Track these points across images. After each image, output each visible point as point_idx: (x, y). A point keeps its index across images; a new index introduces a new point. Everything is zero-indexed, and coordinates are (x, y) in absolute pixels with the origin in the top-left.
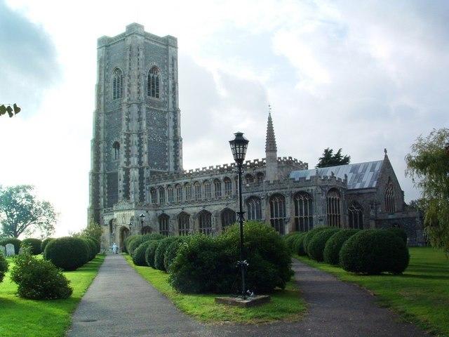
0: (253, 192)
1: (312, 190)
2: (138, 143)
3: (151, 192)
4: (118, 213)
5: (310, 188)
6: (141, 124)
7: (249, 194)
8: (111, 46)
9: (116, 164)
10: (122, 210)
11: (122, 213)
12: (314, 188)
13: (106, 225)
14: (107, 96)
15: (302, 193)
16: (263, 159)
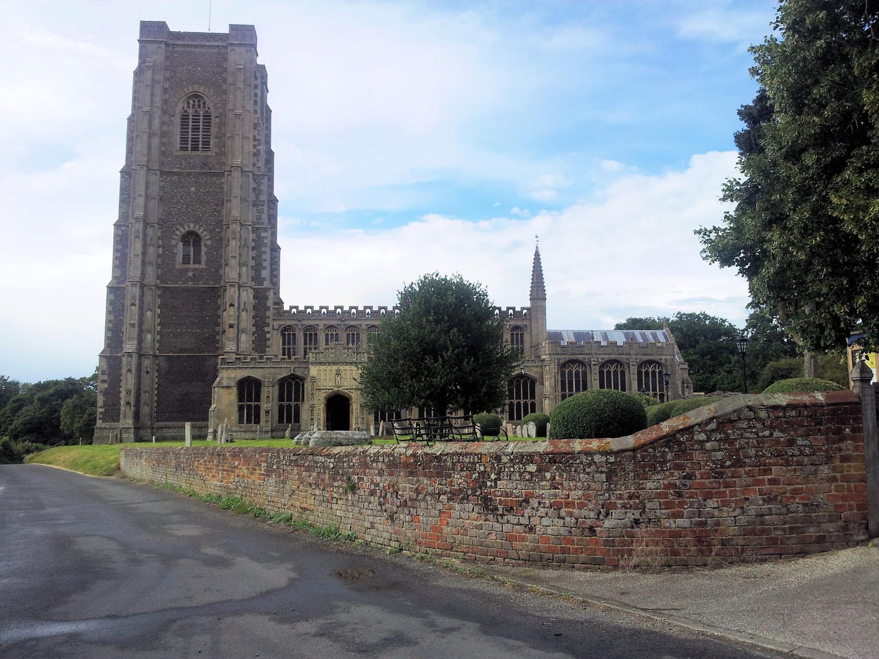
0: (573, 355)
1: (666, 360)
2: (253, 244)
3: (283, 335)
4: (323, 367)
5: (664, 357)
6: (260, 212)
7: (568, 357)
8: (176, 49)
9: (190, 274)
10: (334, 364)
11: (335, 368)
12: (669, 358)
13: (228, 387)
14: (165, 140)
15: (650, 362)
16: (523, 309)
